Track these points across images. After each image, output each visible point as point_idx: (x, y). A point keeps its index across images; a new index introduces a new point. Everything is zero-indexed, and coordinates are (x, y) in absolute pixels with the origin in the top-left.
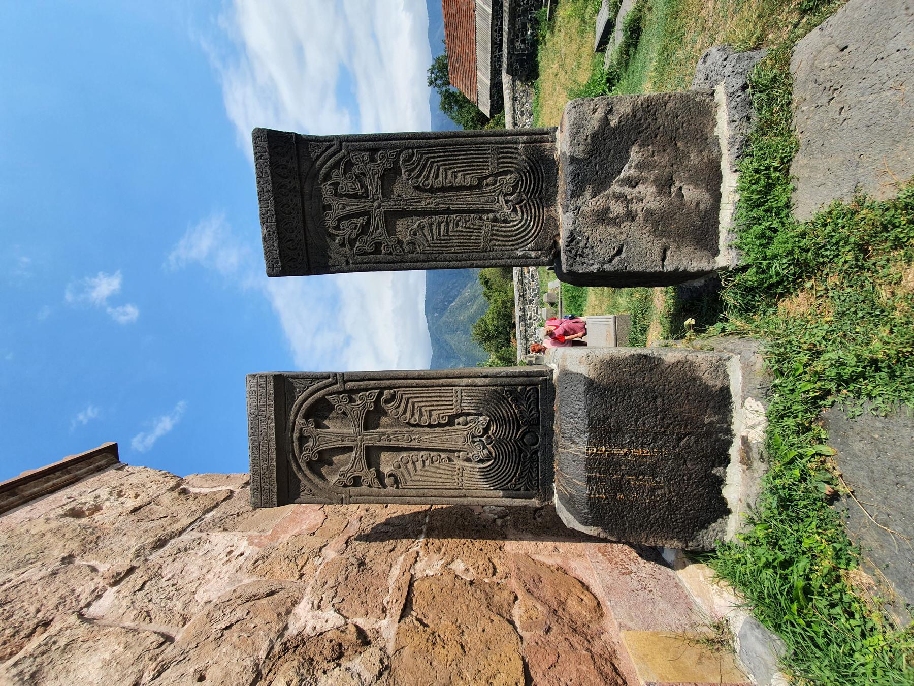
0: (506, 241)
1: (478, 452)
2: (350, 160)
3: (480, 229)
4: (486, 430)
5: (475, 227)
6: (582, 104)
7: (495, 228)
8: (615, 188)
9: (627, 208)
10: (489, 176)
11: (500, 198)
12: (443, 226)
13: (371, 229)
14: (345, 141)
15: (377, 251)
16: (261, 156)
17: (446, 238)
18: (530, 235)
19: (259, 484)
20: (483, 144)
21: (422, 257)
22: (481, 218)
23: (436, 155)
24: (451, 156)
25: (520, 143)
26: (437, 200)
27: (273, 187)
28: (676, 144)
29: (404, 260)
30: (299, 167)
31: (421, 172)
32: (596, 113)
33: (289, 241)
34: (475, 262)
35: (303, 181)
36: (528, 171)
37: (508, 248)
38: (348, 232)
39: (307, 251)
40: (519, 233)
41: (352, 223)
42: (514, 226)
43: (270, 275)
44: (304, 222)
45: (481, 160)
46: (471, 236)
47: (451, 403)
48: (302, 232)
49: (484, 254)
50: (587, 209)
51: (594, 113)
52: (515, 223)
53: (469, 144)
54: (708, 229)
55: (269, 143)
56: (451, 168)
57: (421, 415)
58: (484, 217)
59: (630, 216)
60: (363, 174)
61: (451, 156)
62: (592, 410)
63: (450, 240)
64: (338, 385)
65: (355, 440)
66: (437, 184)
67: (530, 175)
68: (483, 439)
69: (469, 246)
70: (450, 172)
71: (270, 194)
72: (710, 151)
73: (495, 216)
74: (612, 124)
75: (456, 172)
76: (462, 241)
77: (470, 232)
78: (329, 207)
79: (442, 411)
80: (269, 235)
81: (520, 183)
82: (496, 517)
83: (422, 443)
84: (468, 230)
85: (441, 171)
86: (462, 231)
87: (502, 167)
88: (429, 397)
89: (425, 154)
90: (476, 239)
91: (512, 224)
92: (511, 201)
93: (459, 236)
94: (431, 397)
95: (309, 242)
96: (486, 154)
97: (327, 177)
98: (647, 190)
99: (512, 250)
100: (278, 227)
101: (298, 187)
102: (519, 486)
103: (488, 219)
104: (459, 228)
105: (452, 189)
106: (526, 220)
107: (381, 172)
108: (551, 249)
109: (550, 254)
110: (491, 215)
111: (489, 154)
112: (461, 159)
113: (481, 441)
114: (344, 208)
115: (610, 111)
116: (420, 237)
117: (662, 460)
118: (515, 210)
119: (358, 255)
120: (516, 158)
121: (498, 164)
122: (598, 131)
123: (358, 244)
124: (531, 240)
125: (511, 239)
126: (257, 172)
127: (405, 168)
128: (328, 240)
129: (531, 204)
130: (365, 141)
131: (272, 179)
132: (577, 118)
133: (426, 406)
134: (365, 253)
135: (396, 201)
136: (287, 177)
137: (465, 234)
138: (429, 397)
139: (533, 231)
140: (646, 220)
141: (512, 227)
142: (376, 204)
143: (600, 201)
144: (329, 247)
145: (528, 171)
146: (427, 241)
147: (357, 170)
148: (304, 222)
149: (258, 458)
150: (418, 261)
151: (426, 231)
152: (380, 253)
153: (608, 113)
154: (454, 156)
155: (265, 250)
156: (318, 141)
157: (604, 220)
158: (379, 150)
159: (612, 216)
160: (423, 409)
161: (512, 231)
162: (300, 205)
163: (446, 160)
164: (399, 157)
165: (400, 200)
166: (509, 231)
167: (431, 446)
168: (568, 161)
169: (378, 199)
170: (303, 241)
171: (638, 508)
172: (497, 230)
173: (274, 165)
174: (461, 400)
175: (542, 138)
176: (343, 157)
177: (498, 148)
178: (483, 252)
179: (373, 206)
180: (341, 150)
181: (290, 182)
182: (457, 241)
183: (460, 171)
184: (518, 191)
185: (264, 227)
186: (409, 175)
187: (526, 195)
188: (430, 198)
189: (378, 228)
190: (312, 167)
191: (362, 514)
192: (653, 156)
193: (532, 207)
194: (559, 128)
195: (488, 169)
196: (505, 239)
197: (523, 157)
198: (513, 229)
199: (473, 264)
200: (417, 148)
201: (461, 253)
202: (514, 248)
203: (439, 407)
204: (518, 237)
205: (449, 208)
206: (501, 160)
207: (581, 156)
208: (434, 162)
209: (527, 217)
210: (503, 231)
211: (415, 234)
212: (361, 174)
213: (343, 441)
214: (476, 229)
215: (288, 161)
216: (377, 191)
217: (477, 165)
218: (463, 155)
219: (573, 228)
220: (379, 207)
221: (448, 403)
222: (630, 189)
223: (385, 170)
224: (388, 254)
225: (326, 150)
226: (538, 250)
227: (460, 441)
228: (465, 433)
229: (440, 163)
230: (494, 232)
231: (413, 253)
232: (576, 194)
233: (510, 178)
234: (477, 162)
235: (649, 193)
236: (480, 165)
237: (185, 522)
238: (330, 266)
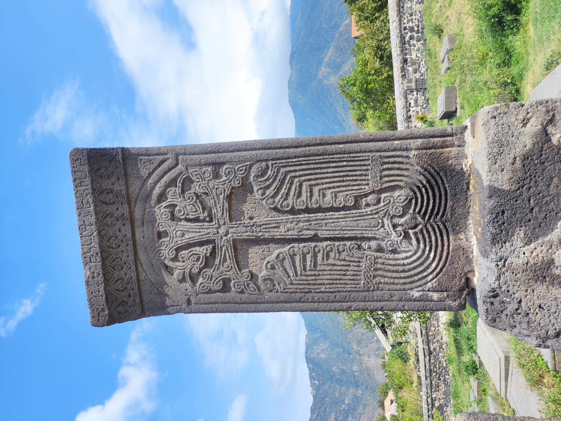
0: (395, 278)
2: (189, 176)
3: (359, 262)
5: (353, 259)
6: (506, 113)
7: (380, 261)
10: (370, 193)
11: (386, 222)
12: (309, 257)
13: (217, 262)
14: (181, 154)
15: (225, 288)
16: (81, 183)
17: (313, 273)
18: (430, 270)
20: (360, 152)
21: (283, 297)
22: (359, 247)
23: (297, 168)
24: (317, 169)
25: (411, 149)
26: (301, 224)
27: (97, 219)
29: (259, 300)
30: (127, 188)
31: (279, 189)
32: (528, 125)
33: (117, 281)
34: (354, 305)
35: (133, 204)
36: (424, 186)
37: (399, 287)
38: (188, 264)
39: (139, 288)
40: (414, 268)
41: (193, 254)
42: (407, 258)
43: (95, 325)
45: (358, 173)
46: (347, 270)
48: (133, 268)
49: (365, 294)
50: (517, 261)
51: (525, 125)
52: (408, 254)
53: (340, 154)
55: (90, 166)
56: (318, 184)
58: (365, 245)
60: (206, 194)
61: (317, 169)
63: (319, 275)
66: (300, 206)
67: (427, 191)
69: (345, 284)
70: (316, 190)
71: (94, 227)
73: (379, 245)
75: (325, 189)
76: (335, 277)
77: (346, 266)
78: (166, 234)
80: (93, 277)
81: (414, 201)
84: (342, 263)
85: (304, 188)
86: (334, 265)
87: (387, 182)
89: (282, 167)
90: (354, 275)
91: (403, 255)
92: (402, 225)
93: (331, 270)
96: (364, 165)
97: (162, 197)
99: (404, 290)
100: (103, 266)
101: (127, 214)
103: (370, 248)
104: (331, 261)
105: (320, 210)
106: (424, 251)
107: (228, 192)
108: (461, 290)
109: (460, 297)
110: (373, 244)
111: (369, 165)
112: (331, 172)
114: (183, 235)
115: (551, 121)
116: (279, 271)
118: (406, 236)
119: (202, 293)
120: (407, 169)
121: (381, 178)
122: (531, 150)
123: (201, 280)
124: (431, 277)
125: (403, 275)
126: (78, 202)
127: (257, 185)
128: (165, 274)
129: (430, 229)
130: (206, 153)
131: (95, 209)
132: (498, 132)
134: (210, 291)
135: (247, 227)
136: (113, 203)
137: (339, 268)
139: (434, 265)
141: (403, 259)
142: (222, 231)
143: (539, 249)
144: (166, 283)
145: (424, 186)
146: (289, 276)
147: (196, 188)
148: (136, 254)
150: (278, 302)
151: (287, 264)
152: (229, 291)
153: (547, 124)
154: (321, 168)
155: (88, 295)
156: (149, 155)
157: (545, 277)
158: (223, 164)
161: (404, 265)
162: (129, 235)
163: (310, 174)
164: (249, 172)
165: (253, 225)
166: (400, 265)
168: (486, 192)
169: (224, 224)
170: (134, 279)
172: (383, 264)
173: (97, 191)
175: (445, 141)
176: (181, 173)
177: (381, 157)
178: (364, 291)
179: (218, 233)
180: (177, 164)
181: (117, 209)
182: (329, 277)
183: (330, 188)
184: (411, 211)
185: (87, 267)
186: (263, 194)
187: (423, 218)
188: (292, 222)
189: (225, 260)
190: (143, 186)
193: (432, 234)
194: (469, 127)
195: (368, 184)
196: (394, 275)
197: (417, 167)
198: (406, 262)
199: (350, 307)
200: (271, 160)
201: (335, 292)
202: (407, 286)
204: (412, 272)
205: (316, 235)
206: (386, 173)
207: (506, 187)
208: (295, 177)
209: (425, 246)
210: (391, 265)
211: (273, 268)
212: (203, 193)
214: (354, 262)
215: (113, 184)
216: (223, 214)
217: (353, 180)
218: (333, 167)
220: (226, 235)
223: (233, 188)
224: (239, 292)
225: (159, 165)
226: (442, 291)
229: (303, 178)
230: (379, 266)
231: (271, 291)
233: (400, 195)
234: (352, 176)
236: (357, 180)
238: (168, 307)
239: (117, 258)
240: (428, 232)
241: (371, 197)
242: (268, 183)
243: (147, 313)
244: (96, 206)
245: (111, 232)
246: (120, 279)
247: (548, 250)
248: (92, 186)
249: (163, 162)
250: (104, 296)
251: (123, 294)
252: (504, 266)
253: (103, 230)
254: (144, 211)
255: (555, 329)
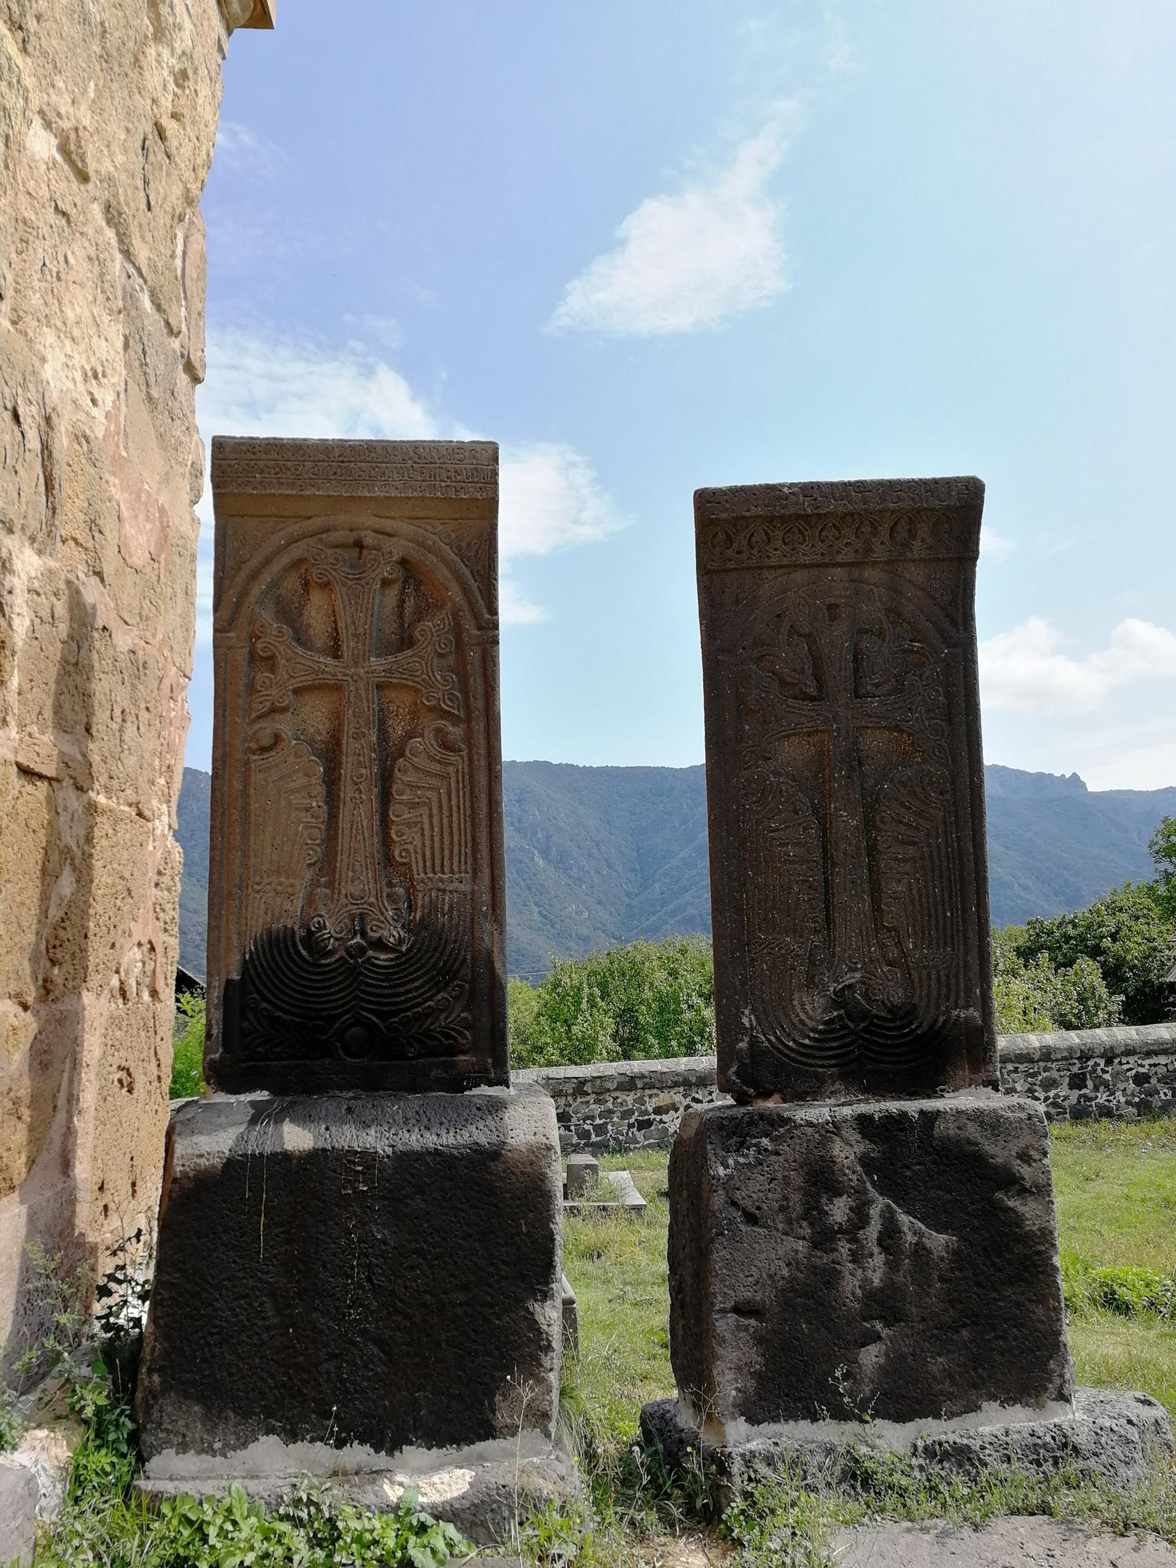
1: (331, 928)
4: (380, 945)
8: (879, 1204)
9: (841, 1231)
11: (858, 975)
19: (264, 457)
28: (965, 1326)
30: (912, 561)
33: (767, 534)
44: (805, 566)
47: (437, 869)
48: (785, 561)
54: (800, 1399)
57: (413, 806)
59: (824, 1238)
62: (438, 1159)
64: (475, 632)
65: (356, 663)
68: (358, 939)
72: (951, 1397)
74: (999, 1195)
79: (420, 851)
82: (123, 974)
83: (350, 805)
88: (451, 822)
94: (451, 827)
95: (766, 574)
98: (876, 1270)
102: (252, 1019)
111: (944, 948)
113: (355, 934)
117: (337, 1308)
121: (925, 967)
124: (773, 1039)
133: (431, 816)
138: (451, 822)
140: (814, 1270)
148: (805, 566)
149: (322, 457)
157: (815, 1184)
159: (824, 1200)
160: (424, 810)
162: (839, 559)
167: (344, 824)
170: (767, 562)
171: (235, 1262)
174: (444, 891)
180: (948, 647)
181: (882, 543)
187: (864, 1030)
191: (140, 653)
192: (942, 1279)
195: (915, 946)
203: (428, 843)
207: (936, 1132)
209: (820, 1032)
213: (356, 635)
215: (923, 540)
219: (799, 1121)
221: (438, 862)
222: (875, 1235)
227: (355, 890)
228: (372, 900)
232: (863, 1122)
235: (869, 1273)
237: (142, 253)
239: (804, 536)
240: (843, 1037)
241: (894, 953)
242: (919, 790)
243: (705, 578)
244: (893, 512)
245: (847, 530)
246: (769, 539)
247: (853, 1188)
248: (925, 509)
249: (954, 623)
250: (748, 514)
251: (745, 543)
252: (828, 1132)
253: (854, 520)
254: (875, 585)
255: (743, 1199)
